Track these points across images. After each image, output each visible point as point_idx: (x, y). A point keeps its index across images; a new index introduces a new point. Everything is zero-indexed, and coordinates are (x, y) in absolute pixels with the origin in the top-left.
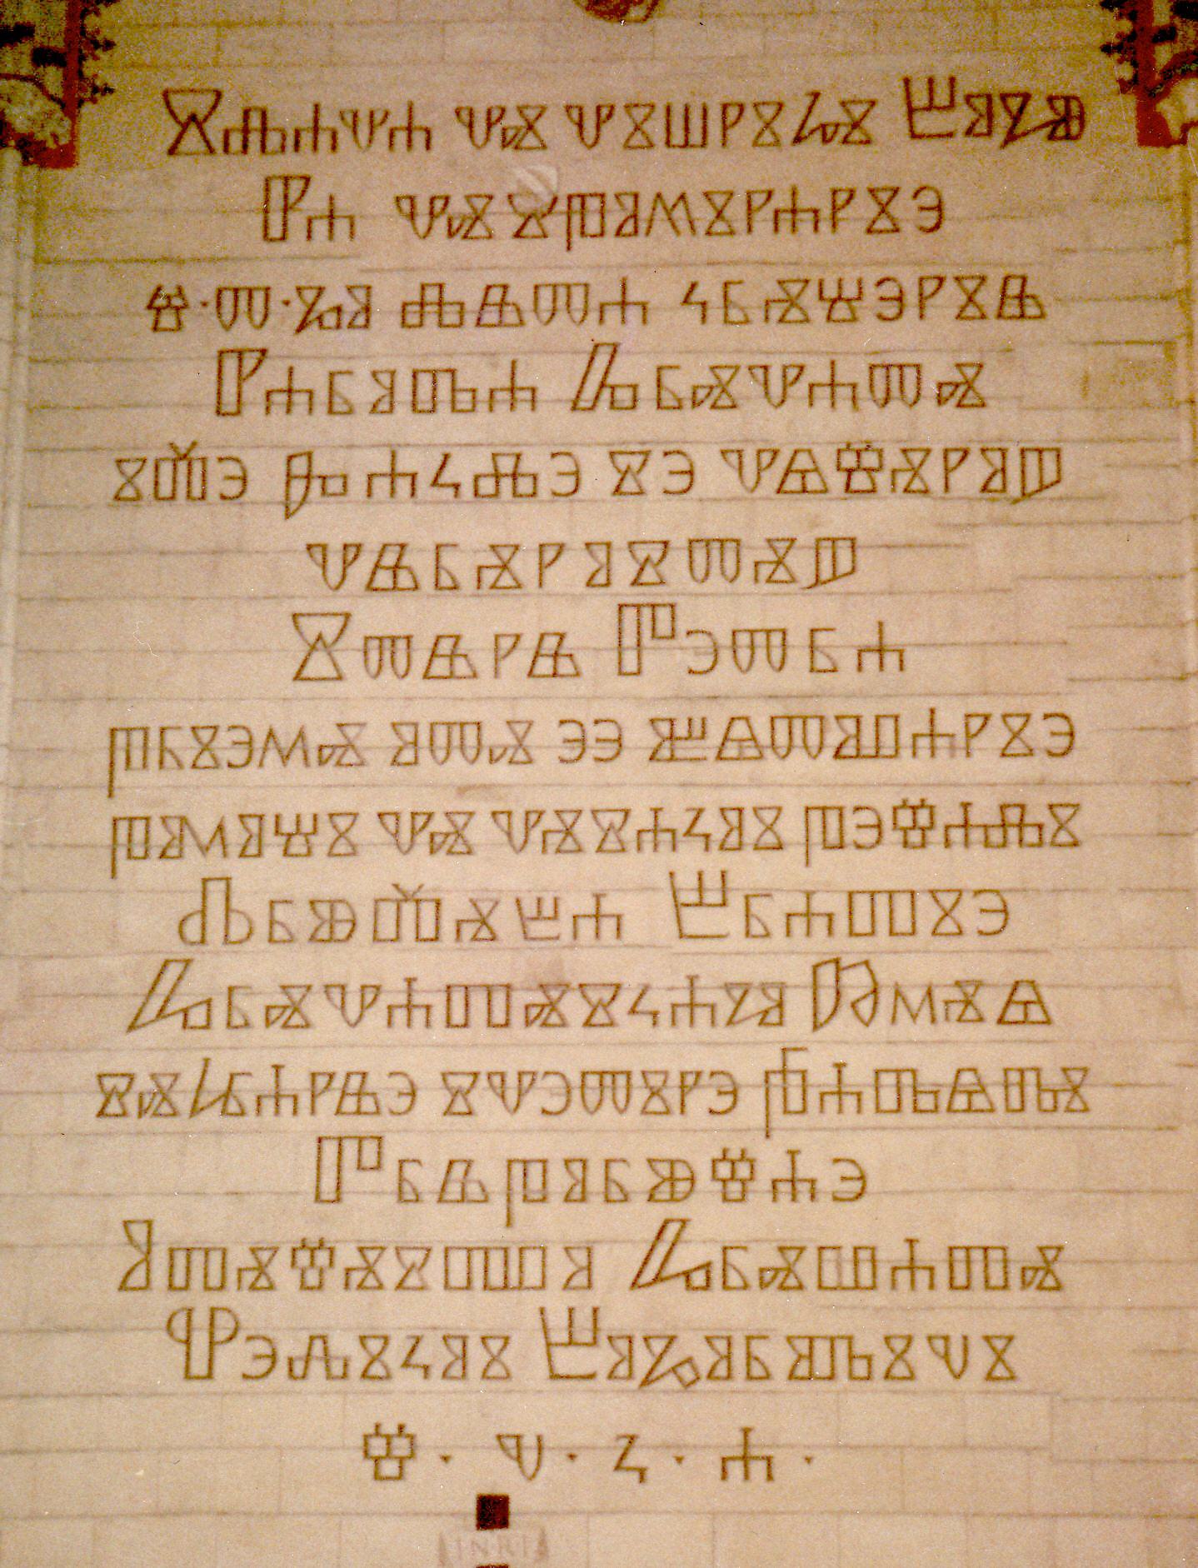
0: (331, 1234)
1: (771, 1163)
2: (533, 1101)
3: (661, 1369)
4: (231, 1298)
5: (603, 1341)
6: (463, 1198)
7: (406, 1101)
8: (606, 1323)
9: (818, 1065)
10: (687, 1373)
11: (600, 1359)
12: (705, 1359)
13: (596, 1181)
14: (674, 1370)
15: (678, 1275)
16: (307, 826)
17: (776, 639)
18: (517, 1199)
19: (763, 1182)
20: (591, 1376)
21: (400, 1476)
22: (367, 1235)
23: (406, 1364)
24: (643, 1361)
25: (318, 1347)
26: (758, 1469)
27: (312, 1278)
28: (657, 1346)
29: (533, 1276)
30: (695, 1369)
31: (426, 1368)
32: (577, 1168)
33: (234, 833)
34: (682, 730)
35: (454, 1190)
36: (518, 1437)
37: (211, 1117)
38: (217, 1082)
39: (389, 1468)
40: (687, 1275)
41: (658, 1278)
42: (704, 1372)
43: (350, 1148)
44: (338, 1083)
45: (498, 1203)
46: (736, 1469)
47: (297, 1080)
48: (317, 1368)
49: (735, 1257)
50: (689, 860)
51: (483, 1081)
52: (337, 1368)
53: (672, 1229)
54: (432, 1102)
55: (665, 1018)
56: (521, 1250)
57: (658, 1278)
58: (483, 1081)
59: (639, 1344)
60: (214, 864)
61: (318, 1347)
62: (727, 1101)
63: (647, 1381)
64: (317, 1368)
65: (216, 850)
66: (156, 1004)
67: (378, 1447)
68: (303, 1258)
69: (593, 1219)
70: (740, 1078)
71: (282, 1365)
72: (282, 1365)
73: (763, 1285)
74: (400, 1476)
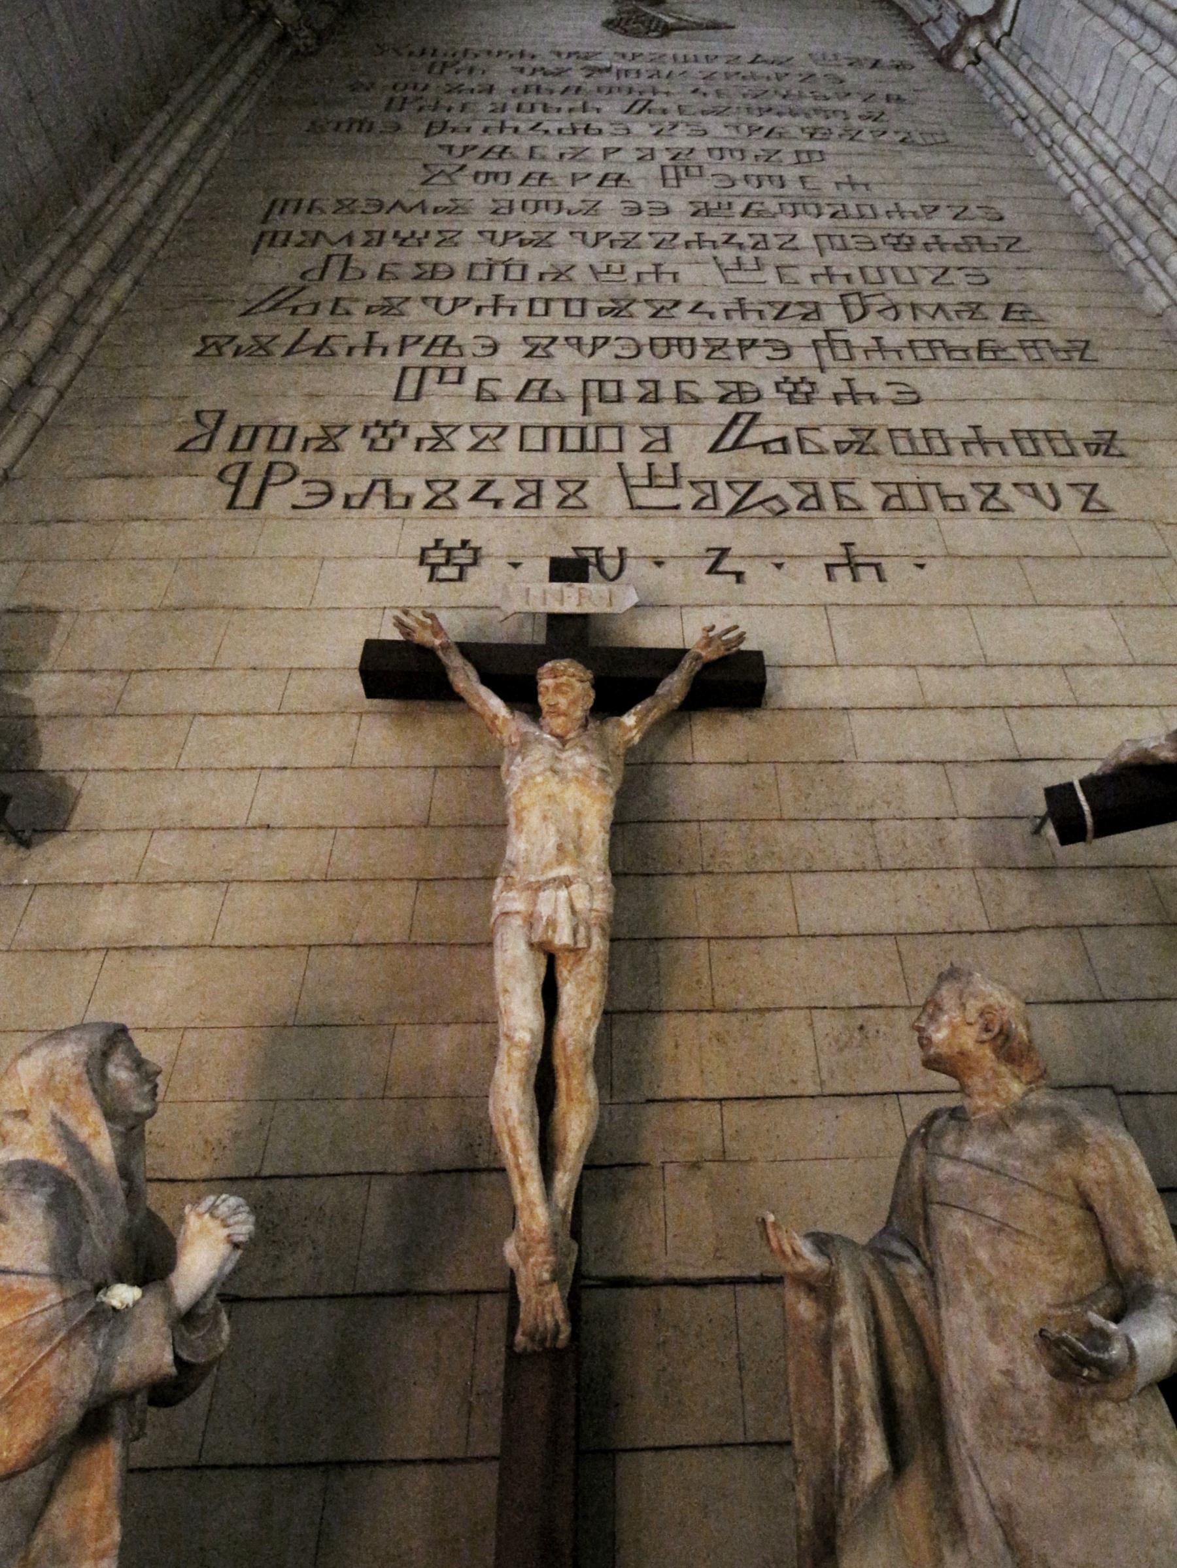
0: (404, 418)
1: (830, 383)
2: (604, 354)
3: (747, 503)
4: (295, 456)
5: (684, 482)
6: (541, 398)
7: (491, 350)
8: (686, 472)
9: (860, 337)
10: (776, 506)
11: (686, 496)
12: (793, 497)
13: (668, 391)
14: (761, 503)
15: (755, 445)
16: (420, 234)
17: (776, 179)
18: (594, 401)
19: (825, 392)
20: (677, 507)
21: (461, 578)
22: (442, 420)
23: (475, 498)
24: (728, 499)
25: (380, 488)
26: (869, 574)
27: (383, 443)
28: (744, 489)
29: (610, 439)
30: (782, 502)
31: (497, 503)
32: (651, 386)
33: (360, 237)
34: (713, 205)
35: (532, 394)
36: (598, 550)
37: (307, 356)
38: (316, 337)
39: (451, 572)
40: (765, 444)
41: (737, 445)
42: (794, 505)
43: (433, 375)
44: (428, 340)
45: (576, 405)
46: (843, 574)
47: (389, 335)
48: (377, 502)
49: (805, 434)
50: (727, 255)
51: (561, 340)
52: (398, 501)
53: (744, 420)
54: (512, 352)
55: (720, 315)
56: (597, 428)
57: (737, 445)
58: (561, 340)
59: (722, 486)
60: (344, 249)
61: (380, 488)
62: (784, 353)
63: (735, 510)
64: (377, 502)
65: (344, 243)
66: (271, 303)
67: (437, 556)
68: (376, 432)
69: (668, 412)
70: (790, 342)
71: (338, 501)
72: (338, 501)
73: (840, 452)
74: (461, 578)
